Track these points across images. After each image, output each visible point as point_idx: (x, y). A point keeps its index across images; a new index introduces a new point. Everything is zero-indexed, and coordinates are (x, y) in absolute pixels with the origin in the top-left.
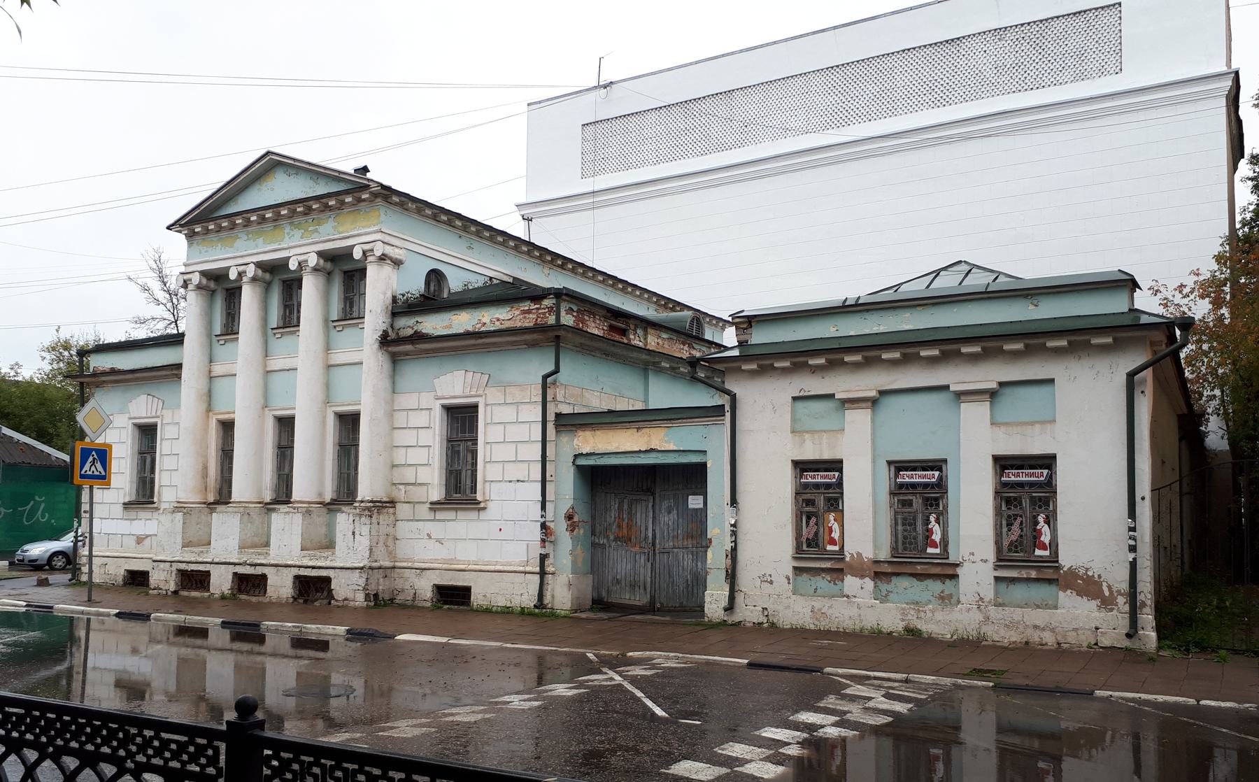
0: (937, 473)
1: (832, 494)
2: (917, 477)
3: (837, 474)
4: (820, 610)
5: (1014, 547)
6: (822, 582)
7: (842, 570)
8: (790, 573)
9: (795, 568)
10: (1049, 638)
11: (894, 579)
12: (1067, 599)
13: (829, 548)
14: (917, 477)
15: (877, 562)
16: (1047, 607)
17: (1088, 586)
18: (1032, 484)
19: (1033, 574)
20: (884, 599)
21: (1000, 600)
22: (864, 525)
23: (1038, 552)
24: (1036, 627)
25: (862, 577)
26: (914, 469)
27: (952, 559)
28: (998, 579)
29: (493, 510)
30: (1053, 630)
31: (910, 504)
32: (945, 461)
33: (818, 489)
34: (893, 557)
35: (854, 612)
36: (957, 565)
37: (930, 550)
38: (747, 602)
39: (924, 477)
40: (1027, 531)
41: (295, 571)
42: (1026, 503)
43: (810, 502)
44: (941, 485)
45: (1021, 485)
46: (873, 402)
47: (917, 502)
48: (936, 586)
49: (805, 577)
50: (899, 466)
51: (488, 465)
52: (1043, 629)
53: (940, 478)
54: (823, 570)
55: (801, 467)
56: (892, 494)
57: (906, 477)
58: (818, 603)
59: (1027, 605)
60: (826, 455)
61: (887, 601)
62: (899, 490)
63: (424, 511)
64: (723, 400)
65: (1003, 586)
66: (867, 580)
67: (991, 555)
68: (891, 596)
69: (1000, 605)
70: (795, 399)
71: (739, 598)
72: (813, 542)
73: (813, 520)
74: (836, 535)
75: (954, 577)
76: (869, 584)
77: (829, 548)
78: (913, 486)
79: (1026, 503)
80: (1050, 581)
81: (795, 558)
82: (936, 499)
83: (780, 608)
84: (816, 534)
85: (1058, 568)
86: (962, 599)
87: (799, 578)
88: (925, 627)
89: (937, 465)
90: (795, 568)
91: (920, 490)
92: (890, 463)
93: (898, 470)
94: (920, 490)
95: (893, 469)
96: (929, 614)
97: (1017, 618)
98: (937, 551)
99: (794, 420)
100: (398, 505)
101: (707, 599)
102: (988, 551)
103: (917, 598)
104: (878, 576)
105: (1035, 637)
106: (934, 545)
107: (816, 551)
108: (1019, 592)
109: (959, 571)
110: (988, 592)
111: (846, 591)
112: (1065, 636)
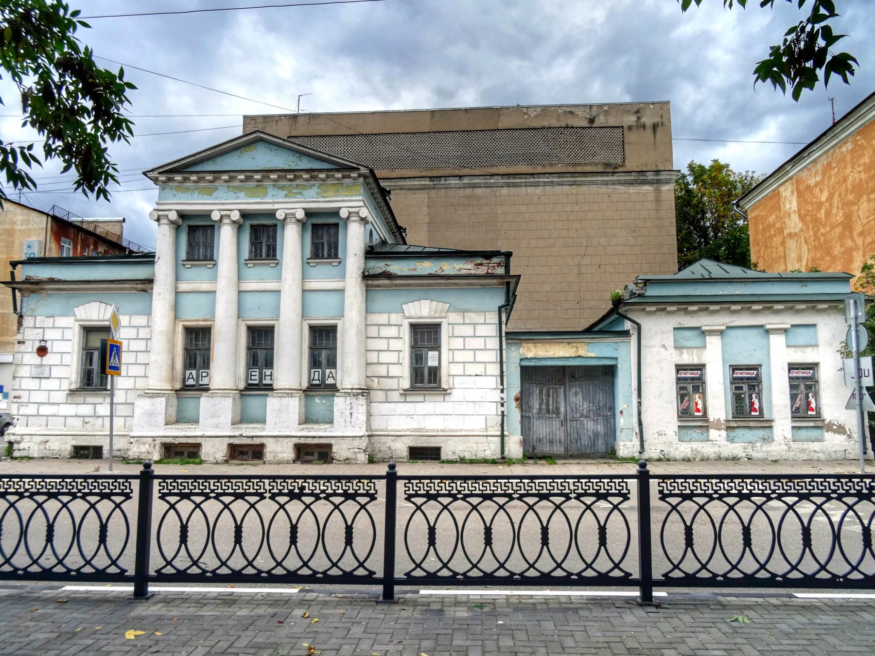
0: (755, 372)
1: (697, 383)
6: (695, 434)
7: (707, 426)
8: (677, 430)
9: (679, 427)
11: (736, 430)
12: (828, 436)
13: (697, 414)
15: (728, 421)
16: (818, 441)
17: (841, 430)
18: (803, 378)
19: (812, 424)
20: (731, 440)
22: (718, 400)
23: (810, 413)
25: (719, 429)
26: (741, 369)
28: (793, 427)
29: (456, 394)
31: (741, 388)
32: (760, 365)
33: (690, 381)
35: (716, 449)
37: (753, 413)
40: (804, 402)
41: (297, 441)
42: (802, 387)
44: (757, 380)
46: (721, 333)
47: (745, 388)
48: (761, 433)
49: (683, 431)
50: (735, 368)
51: (451, 365)
53: (757, 374)
55: (679, 368)
56: (732, 383)
57: (738, 374)
58: (695, 445)
59: (807, 441)
60: (696, 362)
62: (734, 381)
63: (395, 396)
65: (795, 431)
67: (789, 414)
70: (675, 329)
73: (687, 398)
74: (700, 406)
75: (771, 427)
76: (724, 433)
78: (741, 379)
80: (818, 427)
82: (754, 386)
83: (672, 450)
85: (823, 421)
86: (776, 439)
88: (754, 455)
89: (756, 368)
90: (679, 427)
91: (745, 381)
93: (733, 370)
94: (745, 381)
98: (757, 414)
99: (675, 341)
100: (372, 392)
103: (749, 440)
104: (729, 428)
106: (755, 410)
107: (691, 417)
108: (803, 434)
109: (773, 424)
110: (789, 434)
111: (711, 438)
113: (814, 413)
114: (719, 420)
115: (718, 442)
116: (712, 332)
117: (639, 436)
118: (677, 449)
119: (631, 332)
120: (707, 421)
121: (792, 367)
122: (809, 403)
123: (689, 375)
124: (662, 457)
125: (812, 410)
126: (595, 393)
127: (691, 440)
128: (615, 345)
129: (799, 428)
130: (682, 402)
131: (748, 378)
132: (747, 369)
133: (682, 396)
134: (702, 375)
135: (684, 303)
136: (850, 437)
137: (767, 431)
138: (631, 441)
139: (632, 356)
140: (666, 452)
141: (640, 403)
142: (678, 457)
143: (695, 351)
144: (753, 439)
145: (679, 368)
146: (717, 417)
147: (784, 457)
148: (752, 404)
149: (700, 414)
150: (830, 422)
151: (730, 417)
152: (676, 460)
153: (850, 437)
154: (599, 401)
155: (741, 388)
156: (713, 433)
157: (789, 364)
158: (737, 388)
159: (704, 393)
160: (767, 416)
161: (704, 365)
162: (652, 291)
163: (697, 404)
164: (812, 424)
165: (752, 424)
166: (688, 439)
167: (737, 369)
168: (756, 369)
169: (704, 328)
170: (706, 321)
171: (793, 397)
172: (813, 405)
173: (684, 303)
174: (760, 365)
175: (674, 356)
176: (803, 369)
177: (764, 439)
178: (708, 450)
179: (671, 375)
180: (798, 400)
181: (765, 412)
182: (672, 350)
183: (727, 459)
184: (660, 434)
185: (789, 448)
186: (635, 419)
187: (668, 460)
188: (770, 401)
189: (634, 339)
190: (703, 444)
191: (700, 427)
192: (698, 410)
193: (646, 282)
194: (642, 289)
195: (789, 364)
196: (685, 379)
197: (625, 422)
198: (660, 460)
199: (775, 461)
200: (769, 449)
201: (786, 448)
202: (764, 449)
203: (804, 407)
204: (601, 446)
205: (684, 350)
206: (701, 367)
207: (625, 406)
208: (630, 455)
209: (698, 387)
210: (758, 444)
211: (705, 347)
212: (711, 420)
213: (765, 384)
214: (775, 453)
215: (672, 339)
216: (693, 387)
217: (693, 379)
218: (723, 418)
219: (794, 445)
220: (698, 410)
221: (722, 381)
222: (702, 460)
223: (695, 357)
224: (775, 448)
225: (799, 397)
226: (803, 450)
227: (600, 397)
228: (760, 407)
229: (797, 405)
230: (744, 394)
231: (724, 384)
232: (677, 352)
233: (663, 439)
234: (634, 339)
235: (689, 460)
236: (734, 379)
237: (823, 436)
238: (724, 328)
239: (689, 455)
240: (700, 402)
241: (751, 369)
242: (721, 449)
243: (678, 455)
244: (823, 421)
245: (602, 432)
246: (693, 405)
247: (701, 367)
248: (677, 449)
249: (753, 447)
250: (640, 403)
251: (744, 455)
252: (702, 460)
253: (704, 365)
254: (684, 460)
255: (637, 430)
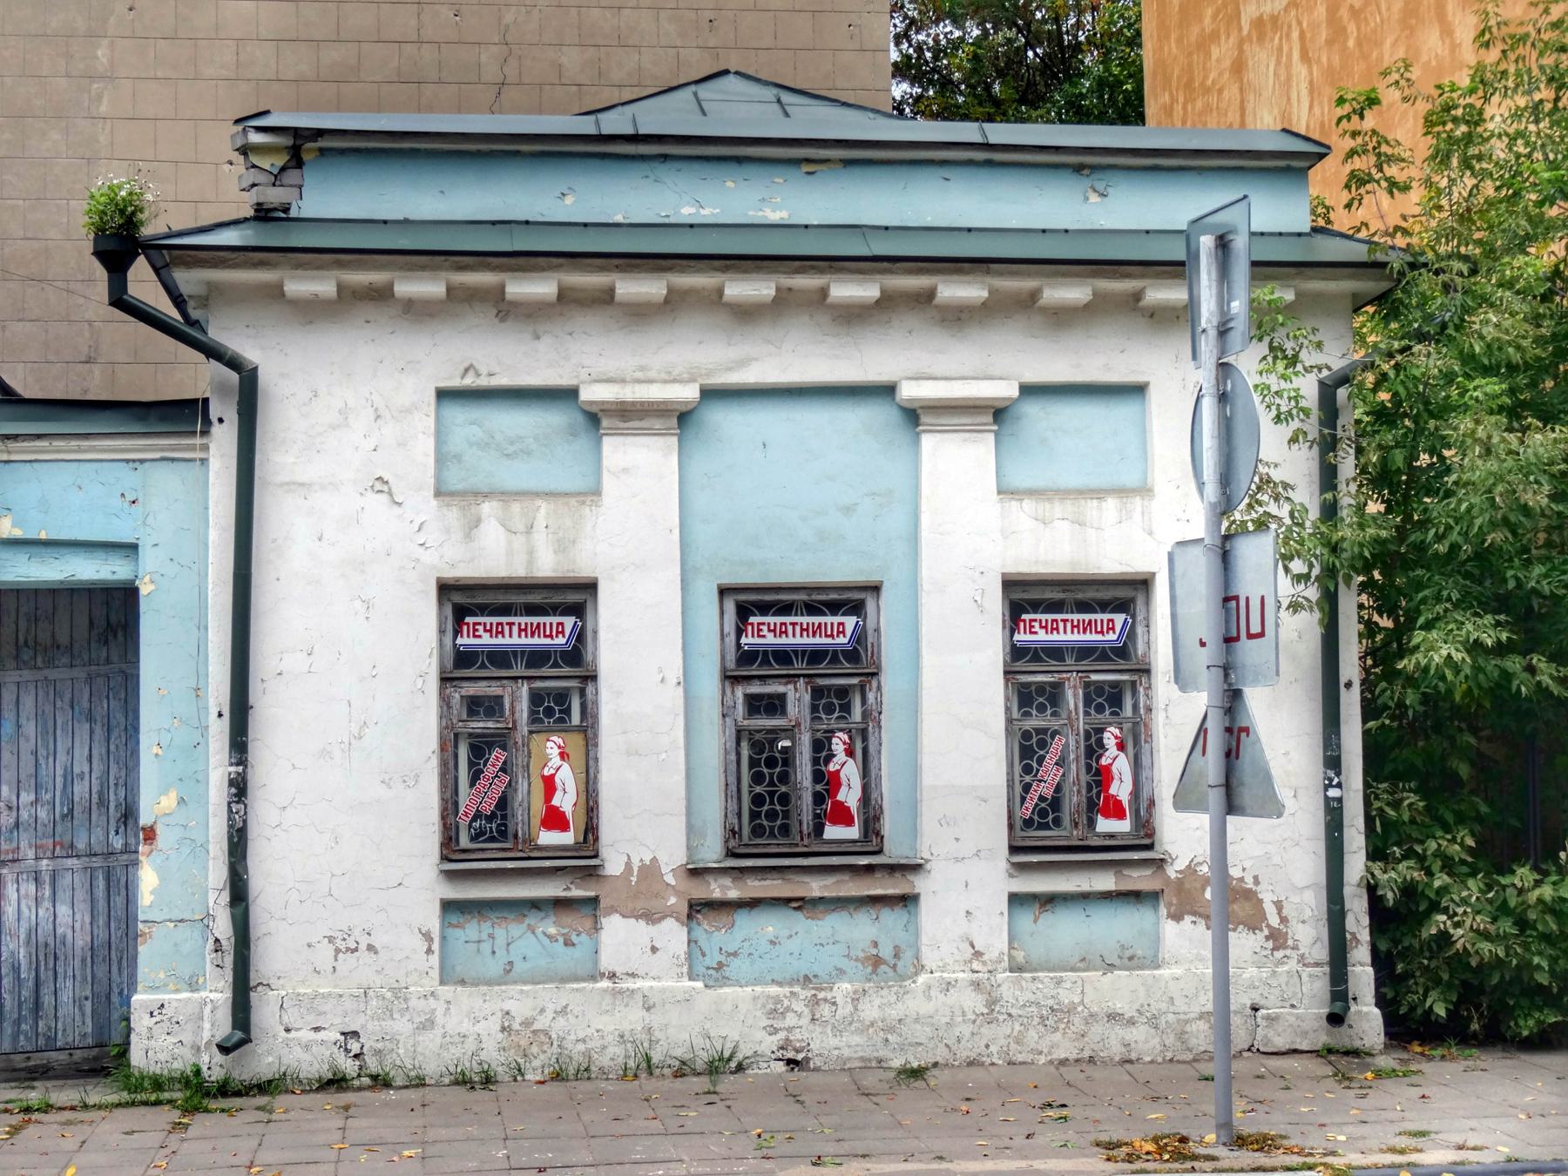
0: (850, 622)
1: (554, 679)
2: (796, 633)
3: (569, 622)
4: (527, 1023)
5: (1048, 812)
6: (532, 941)
7: (594, 901)
8: (432, 920)
9: (448, 906)
10: (1144, 1041)
11: (743, 920)
13: (548, 838)
14: (796, 633)
16: (1132, 962)
18: (1084, 652)
19: (1105, 882)
20: (717, 975)
21: (1020, 956)
23: (1104, 825)
24: (1113, 1017)
25: (651, 917)
26: (786, 609)
27: (894, 850)
28: (1015, 899)
30: (1153, 1022)
32: (875, 589)
33: (514, 655)
34: (731, 854)
35: (632, 1019)
36: (916, 868)
37: (832, 832)
38: (290, 1017)
39: (817, 630)
40: (1076, 770)
42: (1073, 698)
43: (475, 706)
44: (859, 658)
45: (1056, 652)
47: (798, 699)
48: (860, 929)
49: (472, 929)
50: (749, 603)
52: (1131, 1022)
53: (860, 637)
54: (535, 905)
55: (462, 600)
56: (731, 679)
57: (766, 633)
58: (520, 1002)
61: (725, 981)
62: (745, 665)
64: (192, 376)
65: (1026, 919)
66: (670, 924)
68: (736, 967)
69: (1020, 969)
71: (265, 1011)
72: (497, 825)
74: (566, 801)
75: (908, 900)
76: (673, 935)
77: (548, 838)
78: (783, 656)
79: (1073, 698)
80: (1135, 896)
81: (451, 876)
82: (843, 692)
83: (401, 1026)
84: (503, 803)
85: (1160, 864)
86: (929, 957)
87: (457, 934)
89: (851, 600)
90: (448, 906)
91: (800, 667)
92: (723, 592)
93: (743, 612)
94: (800, 667)
95: (730, 607)
96: (845, 1009)
97: (1067, 996)
98: (853, 832)
99: (442, 459)
101: (140, 1022)
102: (989, 828)
103: (804, 968)
105: (1113, 1040)
106: (842, 815)
109: (920, 884)
111: (607, 962)
112: (1181, 1036)
113: (1123, 826)
114: (650, 870)
115: (645, 984)
116: (631, 415)
117: (229, 960)
118: (428, 1024)
119: (214, 411)
120: (592, 874)
121: (1025, 597)
122: (1102, 777)
123: (514, 640)
124: (349, 1067)
125: (1116, 811)
126: (48, 731)
127: (508, 974)
128: (128, 479)
129: (1049, 901)
130: (475, 778)
131: (816, 656)
132: (812, 609)
133: (475, 741)
134: (580, 637)
135: (482, 258)
136: (1278, 939)
137: (891, 918)
138: (193, 986)
139: (213, 535)
140: (368, 1042)
141: (239, 788)
142: (431, 1069)
143: (543, 508)
144: (822, 964)
145: (462, 600)
146: (640, 856)
147: (964, 1053)
148: (828, 783)
149: (567, 838)
150: (1191, 870)
151: (712, 851)
152: (419, 1083)
153: (1278, 939)
154: (69, 778)
155: (775, 705)
156: (620, 937)
157: (1011, 584)
158: (756, 705)
159: (588, 731)
160: (894, 850)
161: (590, 587)
162: (329, 197)
163: (550, 785)
164: (1105, 882)
165: (816, 887)
166: (494, 967)
167: (764, 609)
168: (857, 608)
169: (592, 393)
170: (602, 363)
171: (1028, 749)
172: (1121, 790)
173: (482, 258)
174: (875, 589)
175: (432, 536)
176: (1084, 607)
177: (877, 961)
178: (593, 1025)
179: (418, 639)
180: (1050, 760)
181: (888, 826)
182: (423, 505)
183: (683, 1070)
184: (342, 946)
185: (992, 1003)
186: (217, 873)
187: (381, 1082)
188: (914, 770)
189: (223, 440)
190: (568, 994)
191: (560, 904)
192: (555, 820)
193: (301, 148)
194: (277, 179)
195: (1011, 584)
196: (500, 658)
197: (172, 884)
198: (335, 1082)
199: (916, 1073)
200: (894, 1013)
201: (974, 1002)
202: (870, 1010)
203: (1073, 799)
204: (71, 1017)
205: (487, 508)
206: (573, 598)
207: (169, 802)
208: (181, 1063)
209: (562, 697)
210: (844, 988)
211: (597, 492)
212: (613, 864)
213: (892, 681)
214: (922, 1033)
215: (425, 447)
216: (536, 698)
217: (537, 658)
218: (672, 857)
219: (1010, 988)
220: (555, 820)
221: (675, 671)
222: (558, 1077)
223: (541, 539)
224: (926, 1008)
225: (1056, 745)
226: (1058, 1015)
227: (77, 752)
228: (865, 799)
229: (1046, 790)
230: (790, 732)
231: (687, 681)
232: (453, 515)
233: (360, 970)
234: (223, 440)
235: (488, 1080)
236: (747, 657)
237: (1157, 940)
238: (690, 393)
239: (494, 1055)
240: (566, 777)
241: (834, 608)
242: (655, 1019)
243: (431, 1053)
244: (1160, 864)
245: (82, 941)
246: (529, 801)
247: (573, 598)
248: (428, 1024)
249: (815, 1002)
250: (239, 788)
251: (769, 1043)
252: (558, 1077)
253: (590, 587)
254: (462, 1081)
255: (223, 927)
